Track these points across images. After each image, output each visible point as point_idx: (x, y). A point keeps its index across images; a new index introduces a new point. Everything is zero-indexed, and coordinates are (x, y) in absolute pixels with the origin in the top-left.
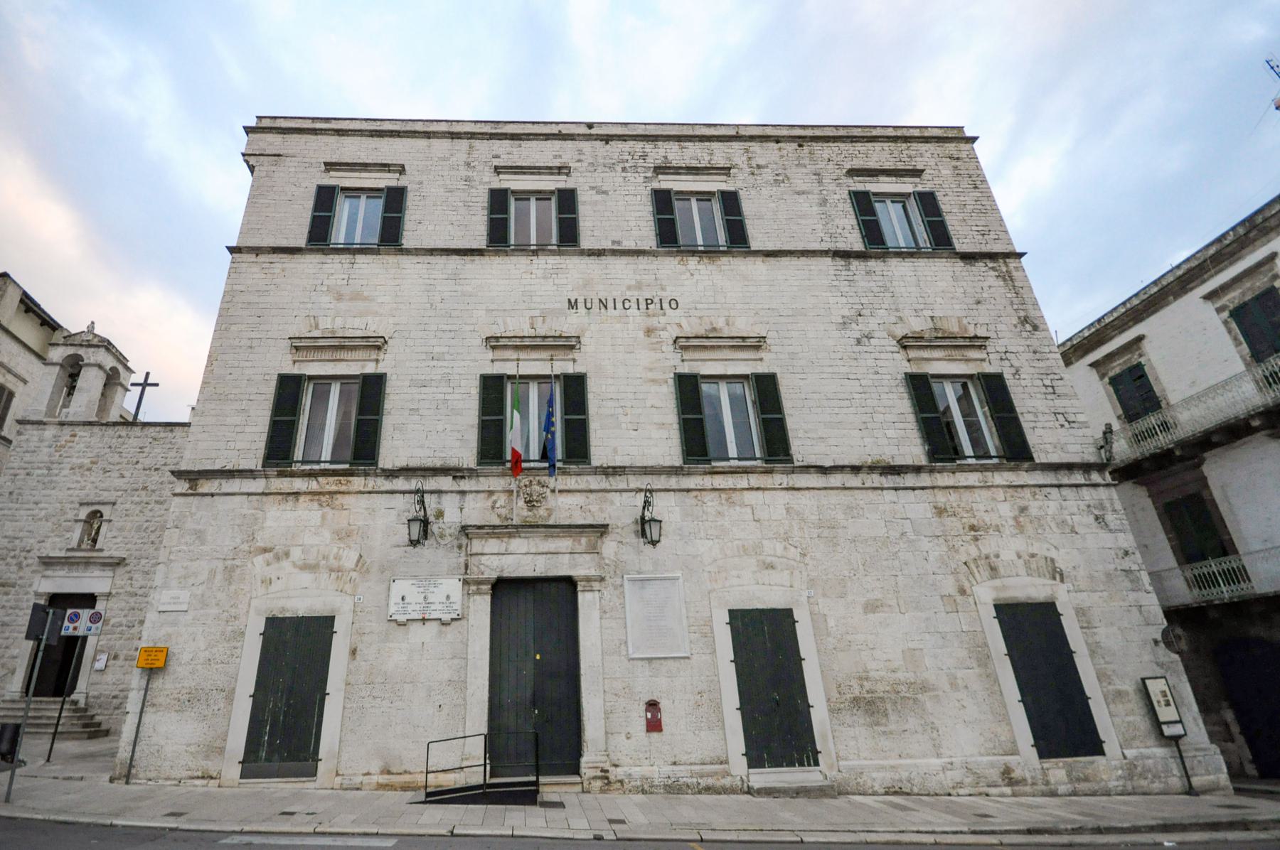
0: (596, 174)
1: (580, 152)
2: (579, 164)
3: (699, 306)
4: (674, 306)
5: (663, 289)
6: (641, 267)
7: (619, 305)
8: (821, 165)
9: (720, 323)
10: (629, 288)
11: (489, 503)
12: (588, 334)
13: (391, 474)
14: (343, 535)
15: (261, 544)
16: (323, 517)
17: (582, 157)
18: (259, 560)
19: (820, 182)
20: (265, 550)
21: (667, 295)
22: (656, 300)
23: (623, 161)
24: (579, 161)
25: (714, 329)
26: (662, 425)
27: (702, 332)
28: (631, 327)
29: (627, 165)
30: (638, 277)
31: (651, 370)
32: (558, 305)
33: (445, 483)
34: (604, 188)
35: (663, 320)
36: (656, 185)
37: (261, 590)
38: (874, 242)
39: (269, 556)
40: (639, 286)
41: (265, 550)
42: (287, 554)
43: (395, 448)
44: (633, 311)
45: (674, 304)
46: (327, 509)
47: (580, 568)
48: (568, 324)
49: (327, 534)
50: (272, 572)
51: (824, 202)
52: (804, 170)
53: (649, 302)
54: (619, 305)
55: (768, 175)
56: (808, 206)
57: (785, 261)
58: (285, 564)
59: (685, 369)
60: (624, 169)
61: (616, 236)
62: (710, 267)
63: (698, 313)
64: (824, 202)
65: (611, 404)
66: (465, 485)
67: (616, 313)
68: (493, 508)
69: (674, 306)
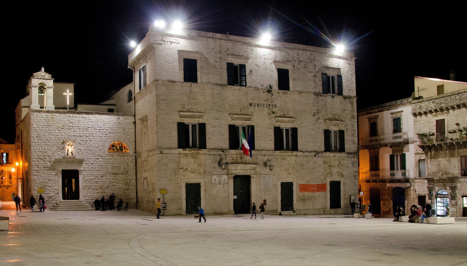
7: (262, 106)
9: (286, 113)
14: (200, 165)
15: (181, 167)
18: (181, 170)
20: (182, 168)
21: (274, 103)
25: (284, 115)
27: (281, 115)
31: (269, 125)
37: (183, 178)
40: (267, 100)
41: (182, 168)
42: (187, 169)
43: (210, 143)
44: (265, 108)
49: (196, 165)
50: (184, 173)
53: (269, 105)
54: (262, 106)
63: (281, 109)
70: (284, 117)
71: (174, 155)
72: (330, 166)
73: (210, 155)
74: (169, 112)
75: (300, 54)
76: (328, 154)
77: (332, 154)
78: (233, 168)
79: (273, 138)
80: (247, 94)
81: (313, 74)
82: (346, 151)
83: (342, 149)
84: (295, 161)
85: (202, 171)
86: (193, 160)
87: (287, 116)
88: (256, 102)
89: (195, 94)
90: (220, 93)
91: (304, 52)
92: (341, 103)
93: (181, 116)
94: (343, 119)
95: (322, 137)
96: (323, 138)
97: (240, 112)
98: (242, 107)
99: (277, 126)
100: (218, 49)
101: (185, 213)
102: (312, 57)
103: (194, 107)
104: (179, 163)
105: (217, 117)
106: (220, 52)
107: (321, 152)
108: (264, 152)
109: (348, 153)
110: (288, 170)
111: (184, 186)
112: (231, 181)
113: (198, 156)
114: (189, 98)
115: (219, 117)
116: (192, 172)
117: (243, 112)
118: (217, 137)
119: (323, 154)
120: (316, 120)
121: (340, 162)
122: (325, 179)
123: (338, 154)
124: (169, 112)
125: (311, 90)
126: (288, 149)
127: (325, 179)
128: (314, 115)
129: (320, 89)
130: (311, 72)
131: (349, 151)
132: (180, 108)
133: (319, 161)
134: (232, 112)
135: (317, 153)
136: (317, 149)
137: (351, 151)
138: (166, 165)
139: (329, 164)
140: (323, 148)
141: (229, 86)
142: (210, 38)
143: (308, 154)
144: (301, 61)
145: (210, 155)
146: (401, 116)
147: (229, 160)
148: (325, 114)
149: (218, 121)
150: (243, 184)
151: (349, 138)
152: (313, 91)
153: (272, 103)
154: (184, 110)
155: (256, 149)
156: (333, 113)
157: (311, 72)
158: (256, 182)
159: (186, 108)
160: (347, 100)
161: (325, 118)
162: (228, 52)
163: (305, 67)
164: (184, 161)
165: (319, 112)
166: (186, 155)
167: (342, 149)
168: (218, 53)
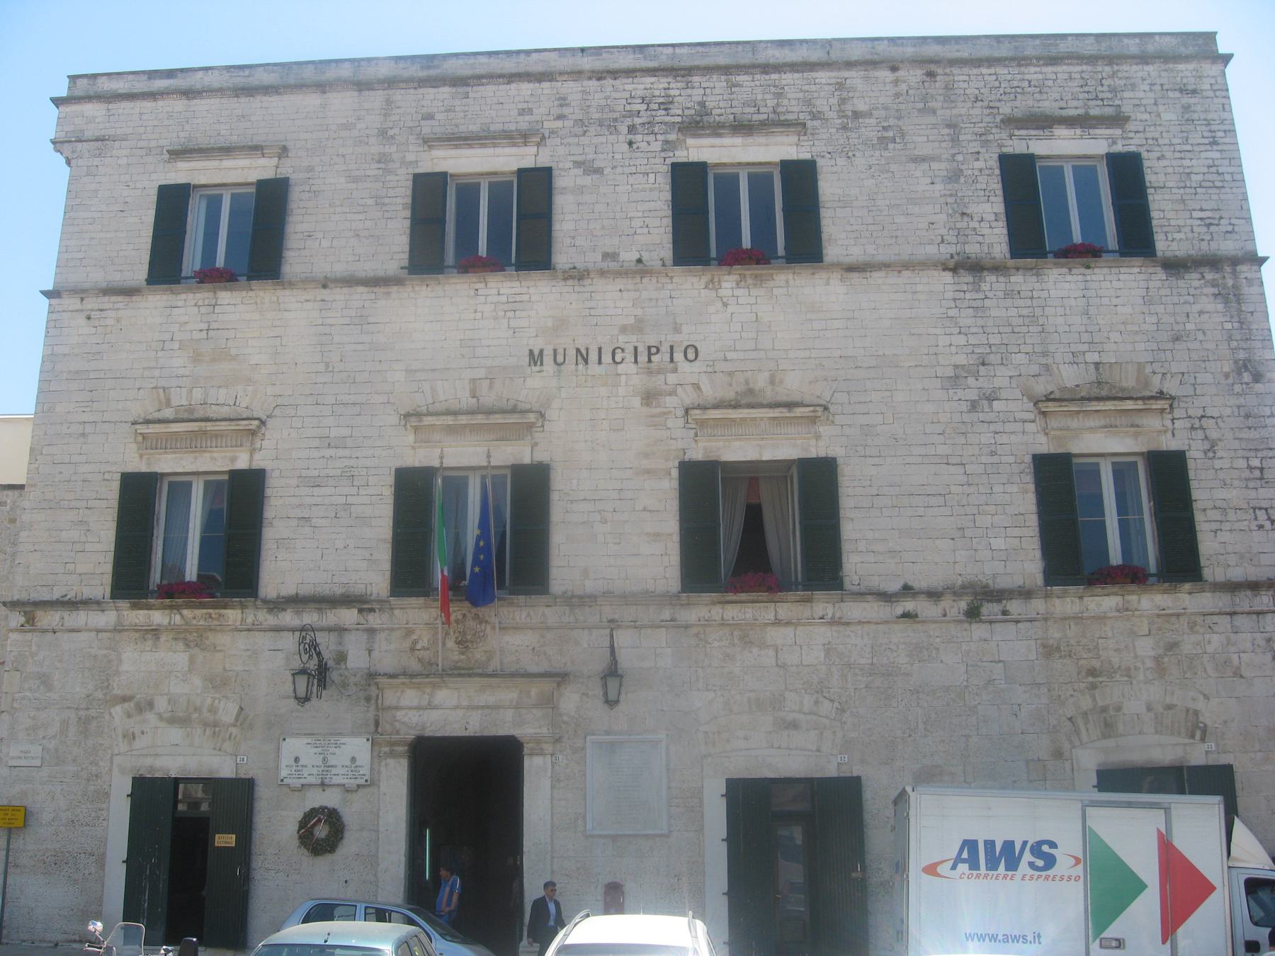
0: (585, 140)
1: (563, 101)
2: (559, 124)
3: (730, 355)
4: (691, 355)
5: (677, 330)
6: (645, 295)
7: (607, 358)
8: (962, 109)
9: (761, 381)
10: (624, 330)
12: (556, 404)
14: (218, 683)
15: (117, 692)
16: (192, 660)
17: (566, 111)
18: (118, 710)
19: (955, 140)
20: (125, 699)
21: (683, 339)
22: (665, 348)
23: (631, 114)
24: (560, 117)
25: (751, 391)
27: (730, 395)
28: (621, 391)
29: (638, 121)
30: (639, 312)
31: (647, 456)
33: (348, 616)
34: (597, 164)
35: (672, 378)
36: (681, 156)
37: (123, 747)
39: (129, 706)
40: (638, 326)
41: (125, 699)
42: (151, 705)
44: (628, 367)
45: (692, 353)
46: (197, 650)
48: (532, 387)
49: (197, 682)
52: (931, 119)
53: (652, 351)
54: (607, 358)
55: (869, 129)
57: (877, 277)
58: (150, 717)
61: (609, 244)
62: (754, 292)
63: (728, 367)
64: (955, 176)
66: (374, 620)
67: (599, 370)
69: (691, 355)
70: (751, 406)
71: (83, 636)
72: (1092, 672)
73: (277, 629)
74: (89, 428)
76: (1069, 602)
77: (1105, 602)
78: (410, 697)
81: (940, 167)
82: (1211, 572)
85: (228, 711)
86: (178, 657)
87: (769, 396)
89: (231, 334)
92: (1148, 301)
94: (1171, 387)
95: (1024, 501)
97: (466, 401)
98: (481, 373)
99: (697, 454)
103: (222, 395)
105: (335, 433)
106: (383, 133)
107: (1025, 594)
111: (121, 789)
113: (212, 638)
114: (197, 358)
115: (346, 432)
116: (173, 721)
117: (488, 398)
118: (326, 539)
119: (1038, 605)
120: (974, 406)
121: (1172, 646)
122: (1058, 754)
123: (1150, 601)
124: (89, 428)
125: (931, 250)
127: (1058, 754)
128: (955, 379)
129: (993, 237)
130: (924, 159)
133: (1010, 642)
135: (981, 600)
138: (45, 681)
144: (857, 115)
145: (277, 629)
147: (388, 654)
148: (1035, 369)
149: (341, 452)
151: (1234, 495)
152: (946, 250)
153: (669, 338)
154: (168, 413)
156: (1093, 357)
157: (924, 159)
158: (555, 780)
159: (175, 402)
161: (1041, 388)
162: (427, 128)
164: (137, 663)
165: (993, 359)
166: (155, 632)
168: (373, 140)
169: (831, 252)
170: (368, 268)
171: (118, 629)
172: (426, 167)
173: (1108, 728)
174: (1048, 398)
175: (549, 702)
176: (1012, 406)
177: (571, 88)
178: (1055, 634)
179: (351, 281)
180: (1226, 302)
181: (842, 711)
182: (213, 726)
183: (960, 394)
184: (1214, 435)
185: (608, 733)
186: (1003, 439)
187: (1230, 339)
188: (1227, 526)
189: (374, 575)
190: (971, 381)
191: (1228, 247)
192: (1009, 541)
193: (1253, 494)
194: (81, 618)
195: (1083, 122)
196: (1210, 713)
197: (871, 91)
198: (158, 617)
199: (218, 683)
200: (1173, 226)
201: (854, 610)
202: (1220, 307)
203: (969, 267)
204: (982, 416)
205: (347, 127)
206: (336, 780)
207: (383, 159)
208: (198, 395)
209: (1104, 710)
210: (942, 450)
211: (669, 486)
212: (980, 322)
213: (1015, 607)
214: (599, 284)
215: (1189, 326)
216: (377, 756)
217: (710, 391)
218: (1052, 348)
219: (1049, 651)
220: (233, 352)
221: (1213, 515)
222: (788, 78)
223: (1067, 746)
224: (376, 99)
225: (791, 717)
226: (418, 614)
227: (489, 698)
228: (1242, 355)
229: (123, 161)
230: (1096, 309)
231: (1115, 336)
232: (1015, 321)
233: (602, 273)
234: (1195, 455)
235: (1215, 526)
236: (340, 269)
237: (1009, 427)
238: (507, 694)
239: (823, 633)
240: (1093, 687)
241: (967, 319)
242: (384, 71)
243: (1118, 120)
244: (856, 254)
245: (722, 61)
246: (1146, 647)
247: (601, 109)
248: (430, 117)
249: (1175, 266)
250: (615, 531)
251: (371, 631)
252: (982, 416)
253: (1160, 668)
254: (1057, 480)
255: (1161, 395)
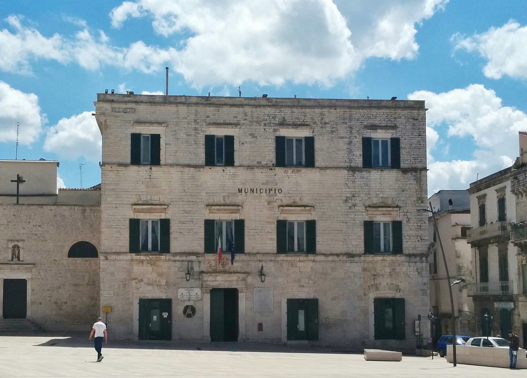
0: (252, 127)
1: (246, 114)
2: (245, 122)
3: (290, 192)
4: (280, 192)
5: (277, 185)
6: (268, 174)
7: (259, 192)
9: (297, 199)
10: (263, 184)
11: (209, 265)
12: (245, 204)
13: (176, 254)
14: (160, 275)
16: (153, 268)
17: (247, 118)
18: (133, 282)
19: (351, 132)
20: (135, 279)
22: (273, 189)
23: (264, 120)
24: (245, 120)
25: (295, 202)
26: (271, 239)
27: (290, 202)
28: (262, 200)
29: (266, 122)
30: (266, 179)
32: (234, 191)
33: (193, 258)
34: (256, 135)
35: (275, 198)
38: (369, 163)
39: (137, 281)
40: (267, 183)
41: (135, 279)
42: (142, 280)
43: (176, 244)
44: (264, 194)
46: (153, 266)
47: (239, 286)
48: (239, 198)
49: (155, 275)
50: (138, 285)
51: (350, 143)
52: (345, 125)
53: (270, 190)
54: (259, 192)
55: (328, 128)
56: (342, 145)
57: (328, 171)
58: (142, 283)
59: (282, 217)
60: (265, 125)
61: (259, 159)
62: (297, 175)
63: (289, 195)
64: (350, 143)
65: (252, 231)
66: (200, 259)
68: (210, 266)
69: (280, 192)
71: (123, 262)
72: (374, 275)
74: (118, 206)
75: (327, 113)
76: (370, 258)
77: (379, 258)
79: (275, 237)
80: (234, 175)
82: (406, 251)
83: (398, 249)
84: (312, 268)
85: (163, 282)
86: (150, 268)
87: (300, 203)
88: (248, 187)
90: (193, 178)
91: (333, 110)
92: (397, 180)
93: (135, 211)
94: (400, 204)
95: (360, 232)
96: (362, 233)
97: (222, 202)
100: (192, 117)
101: (136, 338)
102: (347, 116)
103: (155, 198)
104: (129, 272)
105: (187, 209)
106: (195, 121)
107: (360, 256)
108: (259, 257)
109: (409, 256)
110: (299, 281)
111: (136, 302)
112: (207, 298)
114: (147, 187)
115: (191, 209)
116: (149, 284)
117: (228, 201)
118: (187, 238)
119: (363, 258)
120: (350, 208)
121: (394, 269)
122: (365, 295)
124: (118, 206)
125: (342, 164)
126: (300, 250)
127: (365, 295)
128: (346, 201)
129: (359, 161)
130: (342, 138)
131: (411, 252)
132: (134, 200)
133: (356, 267)
134: (211, 201)
136: (351, 249)
137: (415, 252)
139: (373, 272)
140: (361, 249)
141: (208, 168)
142: (180, 103)
143: (336, 258)
144: (326, 123)
145: (175, 261)
146: (505, 194)
147: (204, 267)
148: (366, 198)
149: (190, 215)
150: (226, 301)
151: (412, 232)
152: (347, 164)
154: (140, 202)
155: (246, 251)
156: (381, 195)
157: (342, 138)
158: (246, 299)
159: (142, 199)
160: (409, 175)
161: (367, 204)
163: (332, 132)
164: (137, 269)
165: (356, 195)
166: (142, 262)
167: (398, 249)
168: (193, 123)
169: (317, 164)
170: (193, 162)
171: (132, 260)
172: (208, 133)
173: (377, 289)
174: (369, 206)
175: (244, 280)
176: (360, 208)
177: (248, 109)
178: (366, 266)
179: (189, 166)
180: (417, 181)
181: (315, 283)
182: (159, 286)
183: (348, 204)
184: (409, 217)
185: (259, 287)
186: (356, 216)
187: (417, 191)
188: (410, 240)
189: (200, 247)
190: (350, 201)
191: (419, 165)
192: (358, 243)
193: (417, 232)
194: (121, 257)
195: (386, 127)
196: (402, 286)
197: (331, 115)
198: (142, 258)
199: (160, 275)
200: (406, 160)
201: (318, 258)
202: (415, 183)
203: (353, 169)
204: (352, 210)
205: (186, 118)
206: (192, 299)
207: (196, 129)
208: (149, 198)
209: (377, 284)
210: (343, 219)
211: (274, 226)
212: (353, 185)
213: (356, 259)
214: (256, 170)
215: (407, 188)
216: (203, 293)
217: (285, 202)
218: (371, 193)
219: (364, 270)
220: (158, 185)
221: (407, 237)
222: (307, 110)
223: (367, 292)
224: (193, 109)
225: (303, 284)
226: (211, 258)
227: (230, 279)
228: (419, 196)
229: (119, 124)
230: (384, 182)
231: (387, 190)
232: (362, 185)
233: (258, 167)
234: (404, 222)
235: (407, 240)
236: (186, 162)
237: (358, 214)
238: (234, 277)
239: (311, 264)
240: (374, 279)
241: (350, 184)
242: (194, 100)
243: (395, 127)
244: (323, 165)
245: (289, 104)
246: (388, 270)
247: (257, 118)
248: (208, 117)
249: (405, 171)
250: (261, 238)
251: (200, 262)
252: (352, 210)
253: (391, 275)
254: (370, 228)
255: (397, 206)
